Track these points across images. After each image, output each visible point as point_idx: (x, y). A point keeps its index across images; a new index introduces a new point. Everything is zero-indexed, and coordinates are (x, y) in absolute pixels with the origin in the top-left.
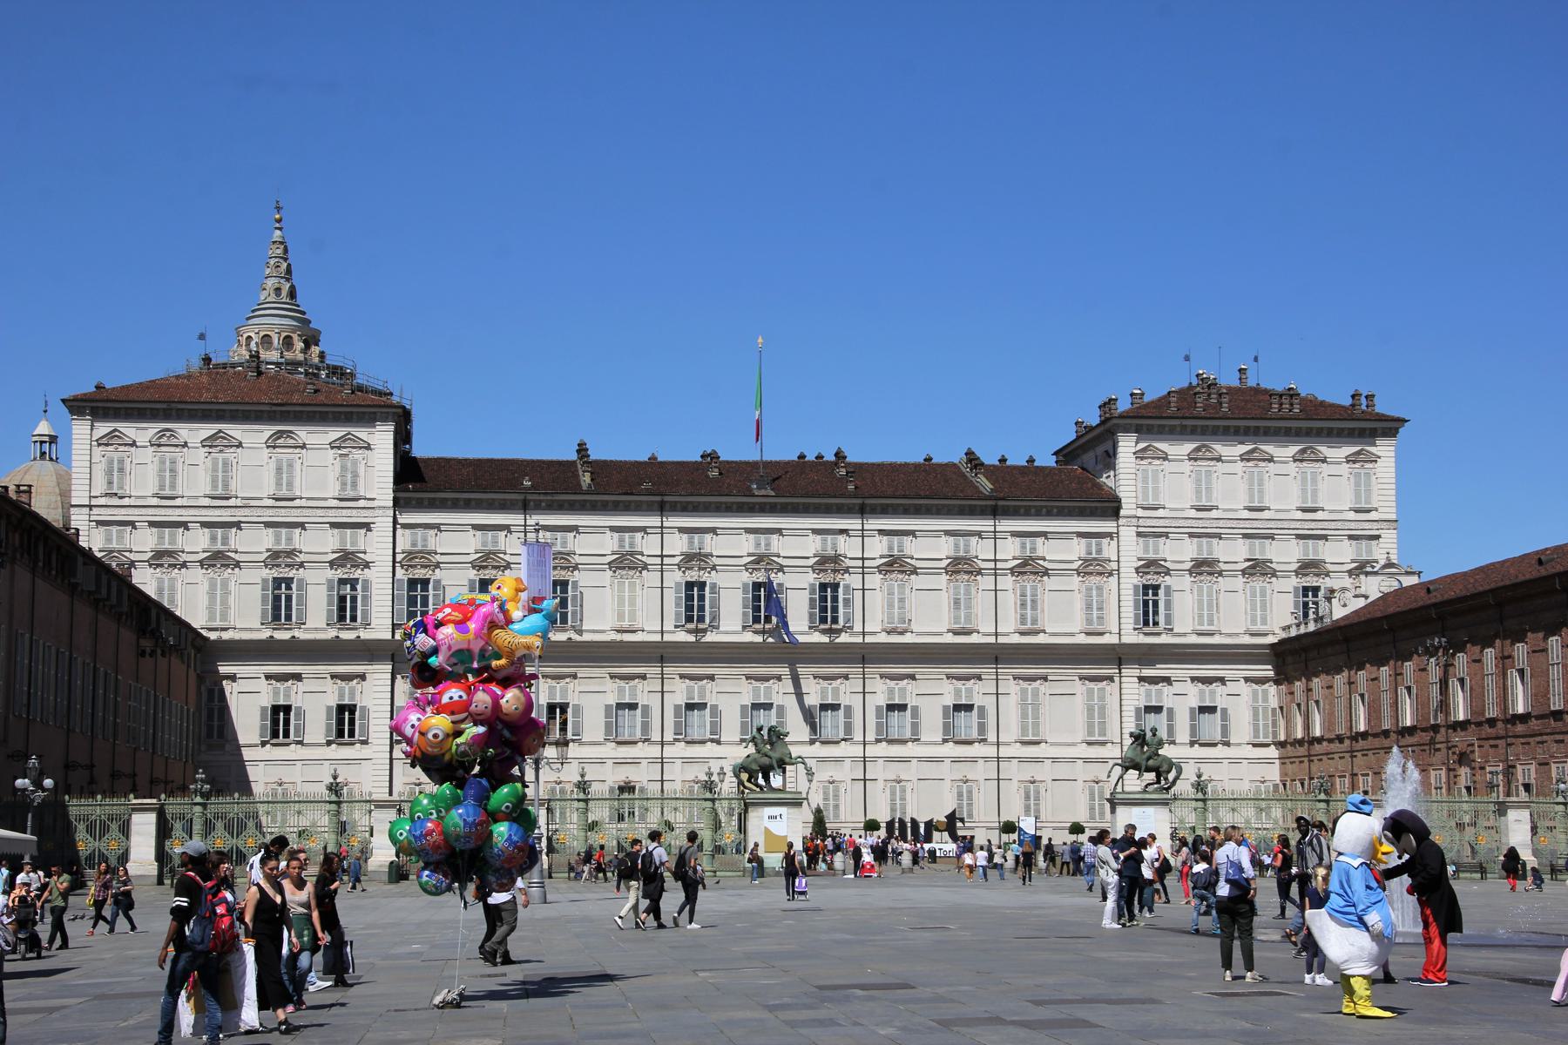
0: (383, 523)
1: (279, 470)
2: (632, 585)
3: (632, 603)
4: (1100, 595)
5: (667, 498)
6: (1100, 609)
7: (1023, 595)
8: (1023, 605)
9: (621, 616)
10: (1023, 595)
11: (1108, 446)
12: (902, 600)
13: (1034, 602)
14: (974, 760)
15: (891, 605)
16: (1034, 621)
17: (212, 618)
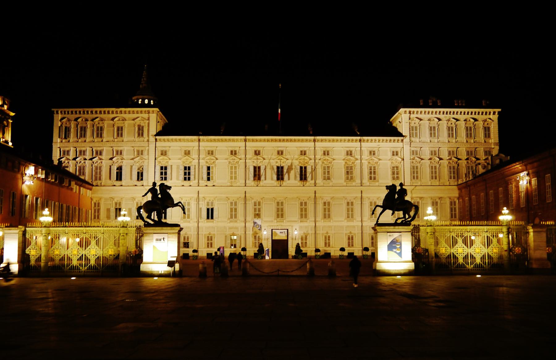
0: (152, 146)
1: (118, 130)
2: (235, 167)
3: (235, 173)
4: (397, 169)
5: (248, 137)
6: (397, 174)
7: (371, 169)
8: (371, 173)
9: (231, 178)
10: (371, 169)
11: (400, 120)
12: (328, 172)
13: (374, 172)
14: (354, 227)
15: (324, 173)
16: (375, 178)
17: (96, 179)
